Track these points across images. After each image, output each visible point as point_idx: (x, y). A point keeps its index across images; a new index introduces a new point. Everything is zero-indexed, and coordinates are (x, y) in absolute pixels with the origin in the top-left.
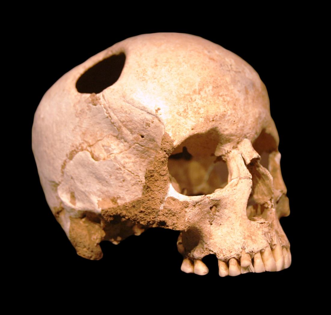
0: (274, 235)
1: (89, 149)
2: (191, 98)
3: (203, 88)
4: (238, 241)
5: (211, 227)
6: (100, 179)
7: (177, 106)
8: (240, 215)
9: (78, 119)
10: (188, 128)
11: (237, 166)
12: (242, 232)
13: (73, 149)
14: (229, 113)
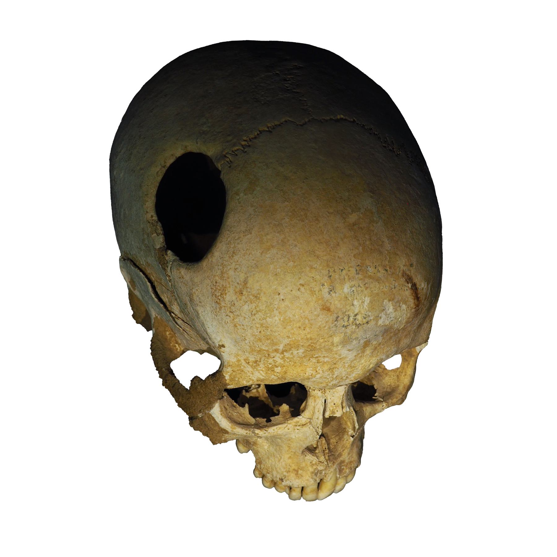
2: (269, 355)
3: (290, 349)
10: (253, 378)
11: (314, 407)
14: (318, 376)
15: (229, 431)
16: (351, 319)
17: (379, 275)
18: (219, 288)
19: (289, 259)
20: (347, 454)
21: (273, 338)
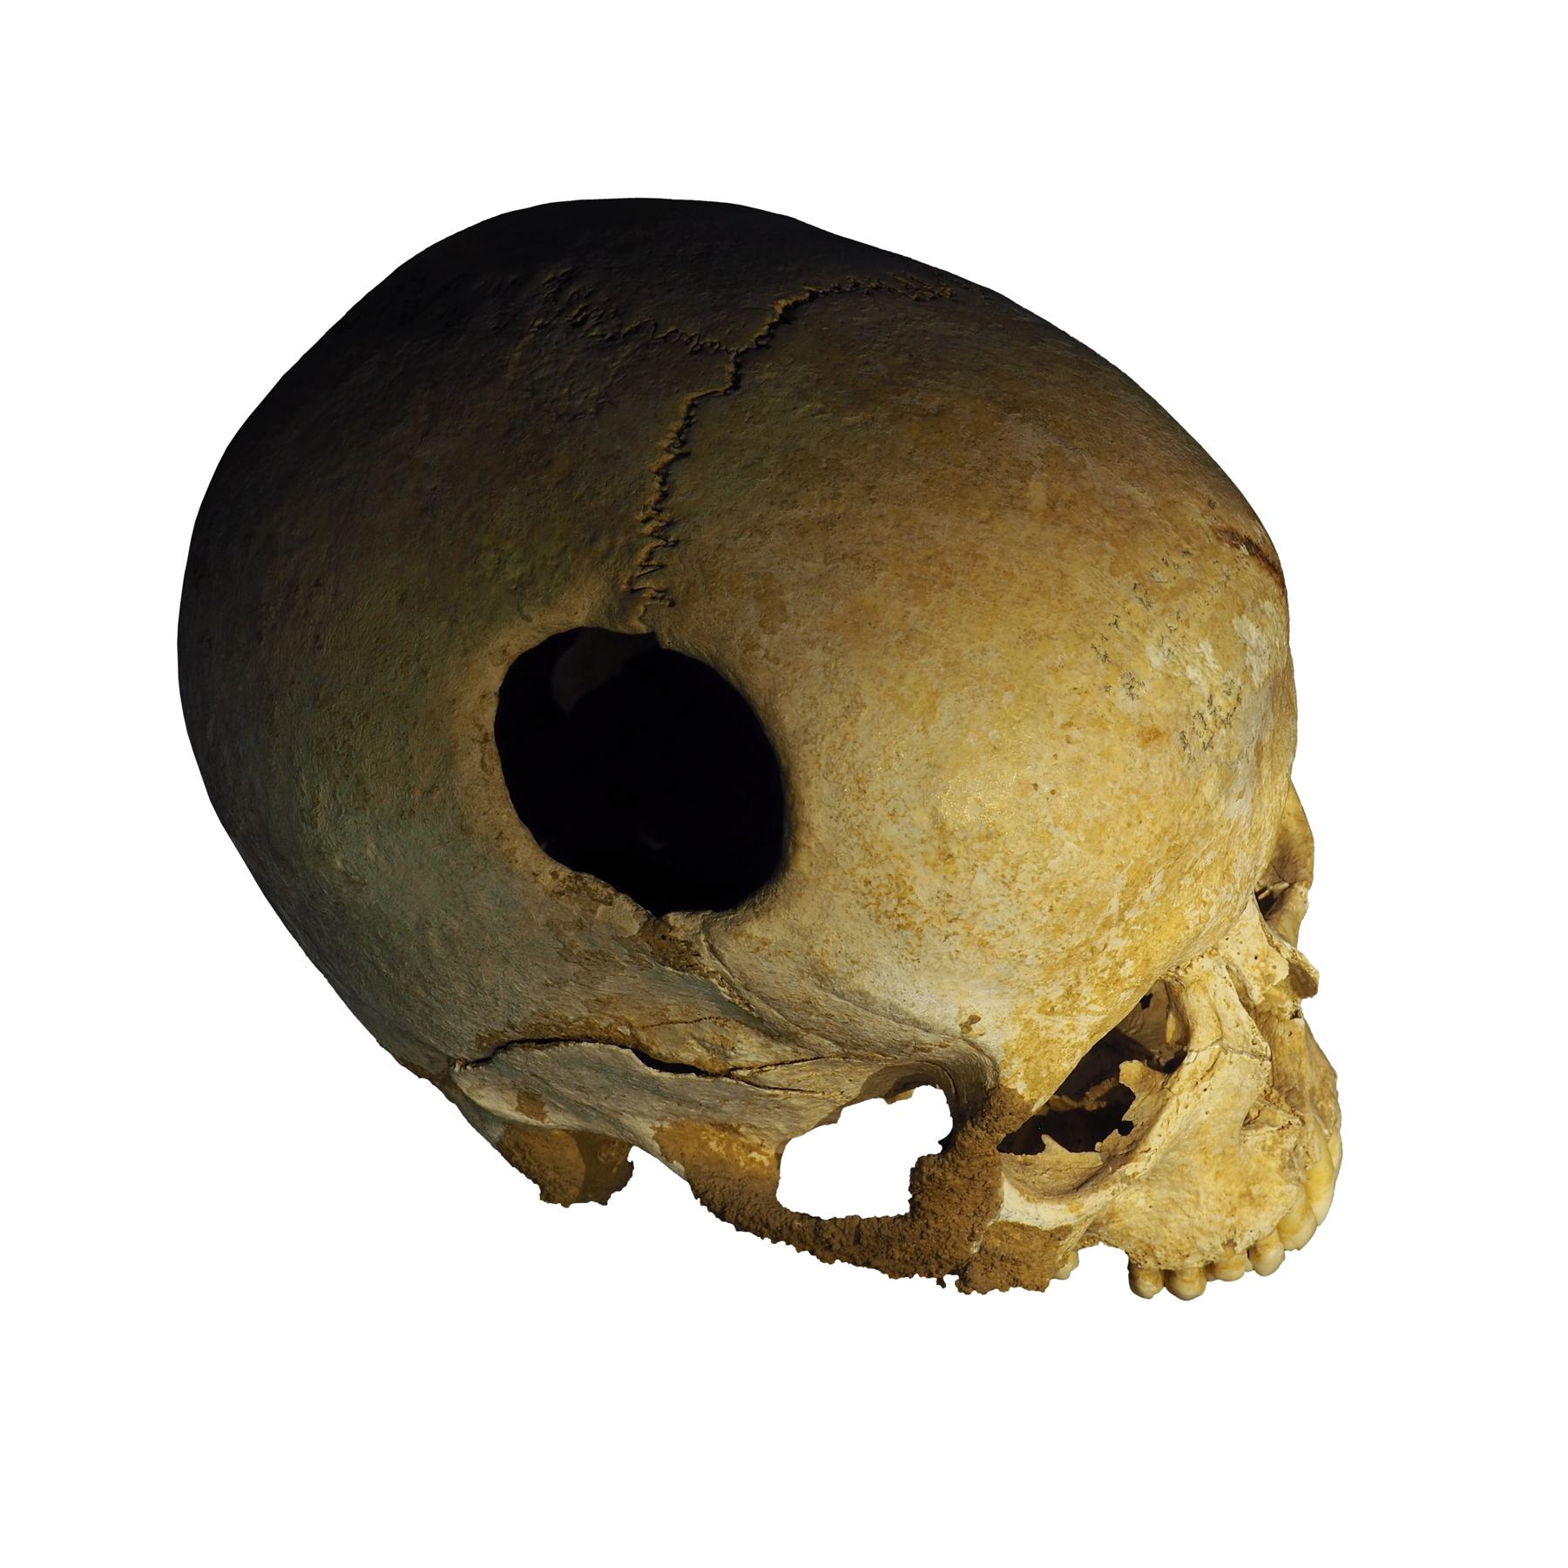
3: (1136, 894)
4: (1212, 1228)
7: (1040, 991)
11: (1213, 1006)
15: (1072, 1223)
16: (1208, 717)
17: (1186, 573)
18: (883, 890)
21: (1086, 898)
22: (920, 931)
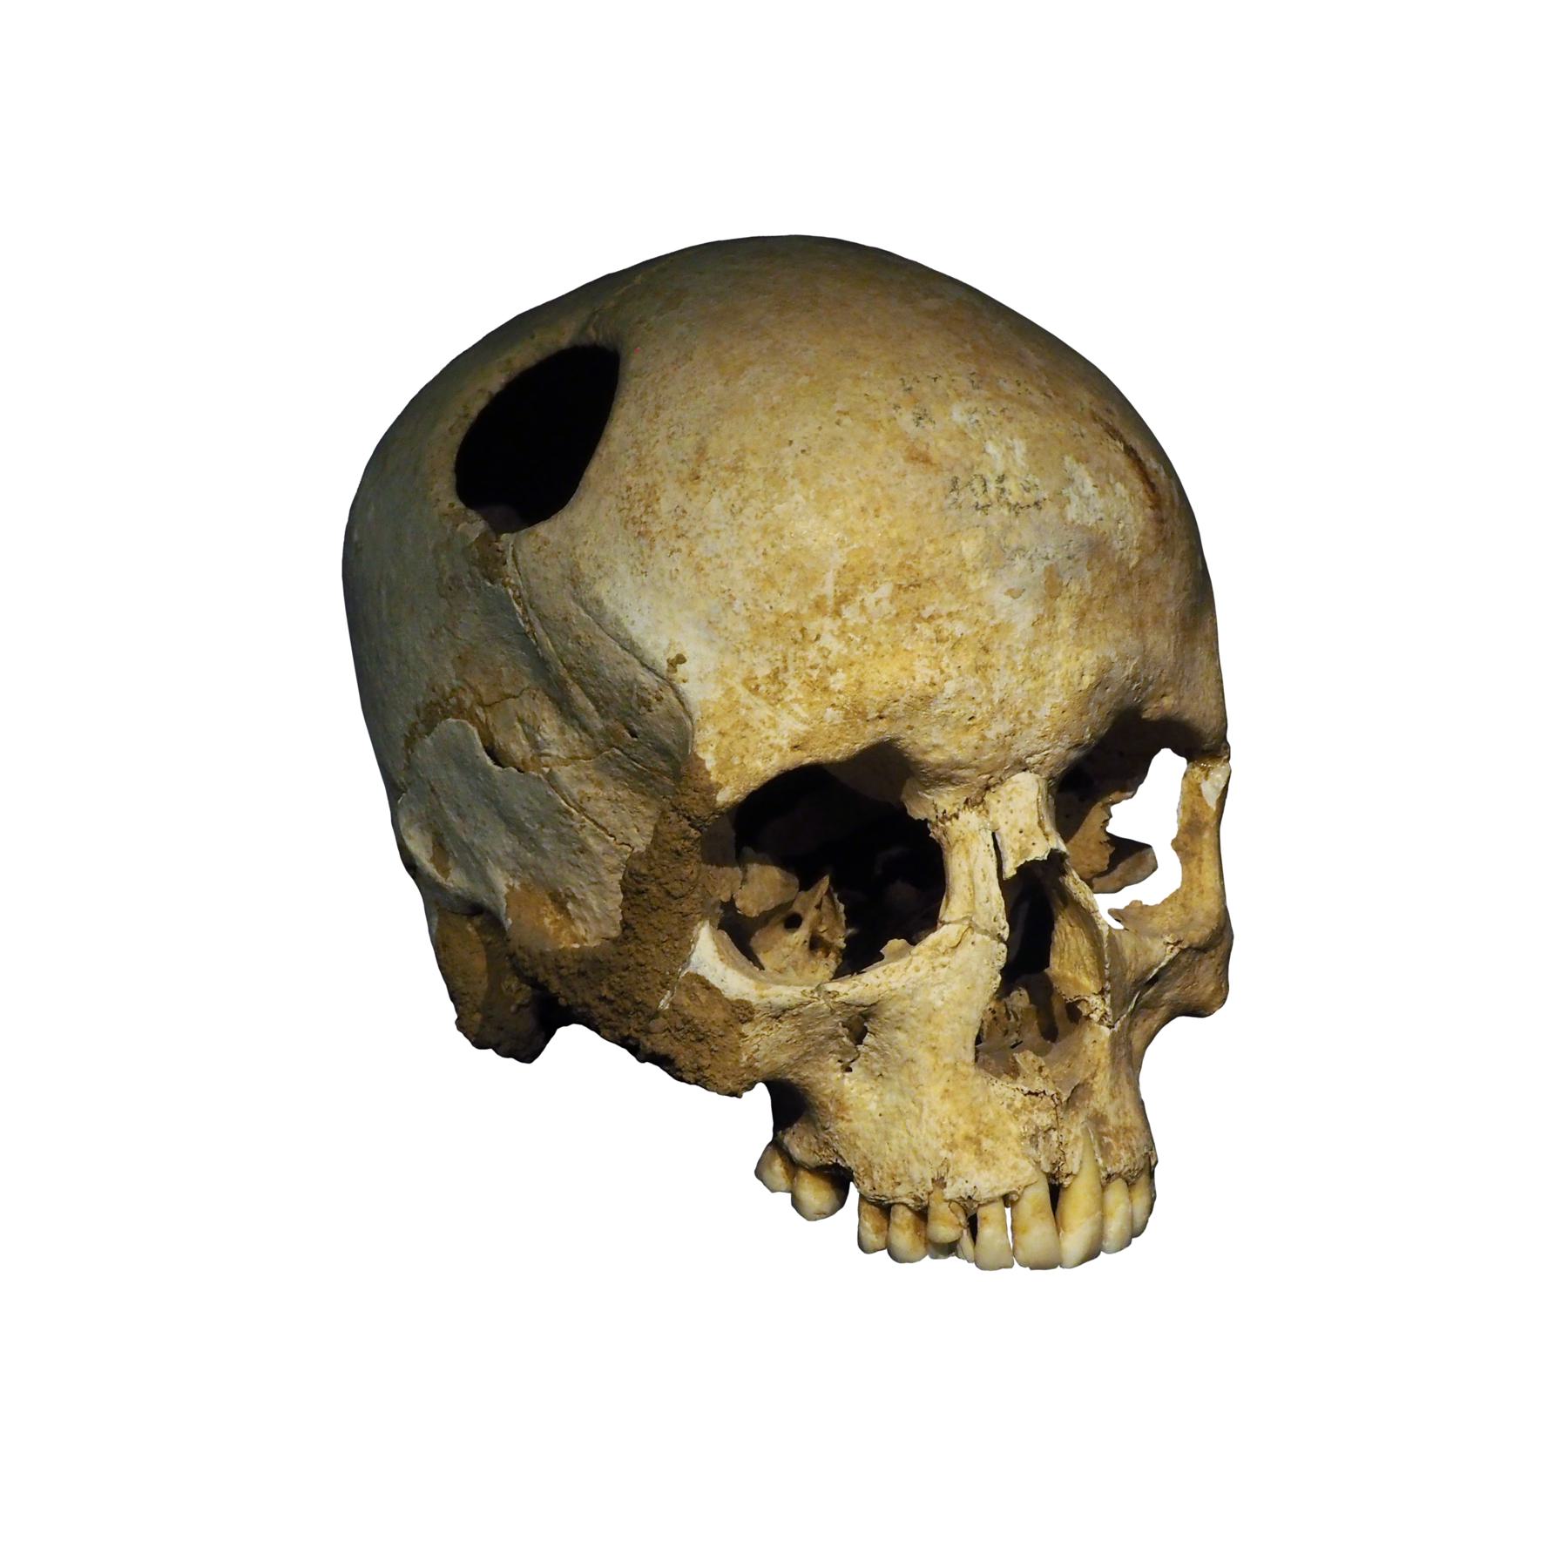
0: (1077, 1138)
1: (479, 711)
2: (803, 630)
4: (926, 1154)
5: (846, 1081)
6: (514, 826)
7: (745, 655)
8: (949, 1060)
9: (444, 603)
10: (778, 741)
11: (971, 875)
12: (946, 1122)
13: (433, 697)
14: (950, 688)
19: (796, 374)
20: (1106, 1092)
22: (653, 540)
